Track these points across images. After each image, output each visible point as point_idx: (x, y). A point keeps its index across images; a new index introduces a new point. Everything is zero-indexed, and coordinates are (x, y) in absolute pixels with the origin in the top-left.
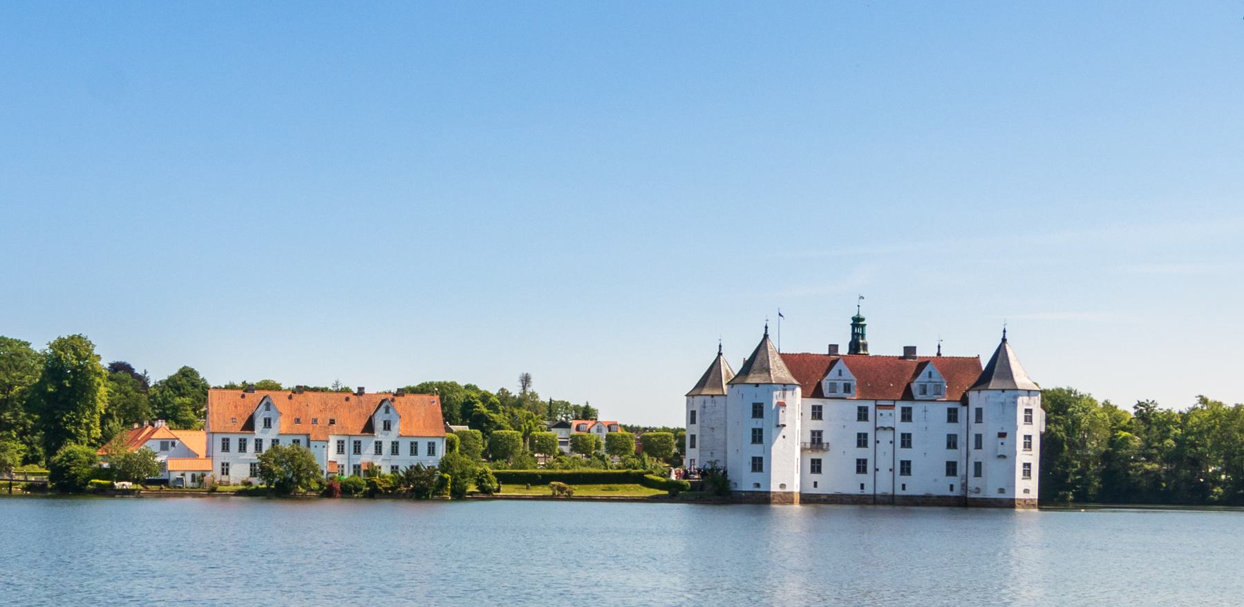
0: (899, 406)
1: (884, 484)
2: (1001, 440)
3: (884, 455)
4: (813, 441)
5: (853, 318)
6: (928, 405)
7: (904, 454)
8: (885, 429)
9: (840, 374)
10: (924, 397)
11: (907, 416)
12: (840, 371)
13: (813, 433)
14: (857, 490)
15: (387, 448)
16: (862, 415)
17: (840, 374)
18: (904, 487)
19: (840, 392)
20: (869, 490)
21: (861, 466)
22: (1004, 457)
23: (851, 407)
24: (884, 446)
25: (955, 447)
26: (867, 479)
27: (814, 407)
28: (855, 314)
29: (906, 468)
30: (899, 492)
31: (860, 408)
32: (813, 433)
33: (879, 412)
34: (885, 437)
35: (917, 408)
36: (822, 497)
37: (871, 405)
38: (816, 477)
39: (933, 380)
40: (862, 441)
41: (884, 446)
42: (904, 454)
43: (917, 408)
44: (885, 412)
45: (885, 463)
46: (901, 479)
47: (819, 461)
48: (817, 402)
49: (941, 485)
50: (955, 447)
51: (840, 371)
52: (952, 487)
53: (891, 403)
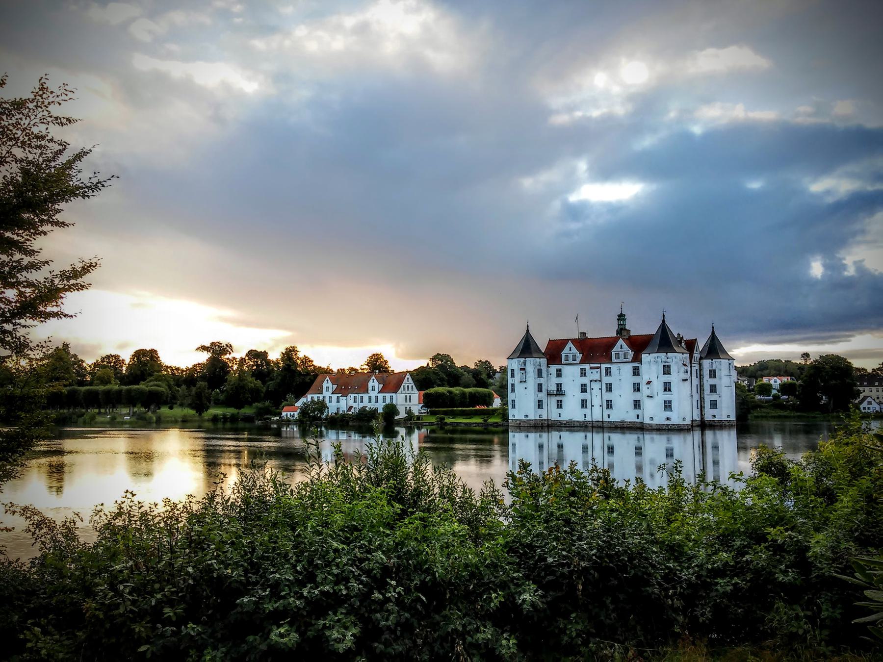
0: (604, 366)
1: (597, 414)
2: (648, 386)
3: (596, 398)
4: (558, 390)
5: (619, 316)
6: (621, 365)
7: (607, 396)
8: (596, 381)
9: (570, 350)
10: (618, 361)
11: (608, 373)
12: (570, 348)
13: (557, 385)
14: (581, 419)
15: (373, 399)
16: (583, 373)
17: (570, 350)
18: (609, 415)
19: (571, 361)
20: (589, 418)
21: (584, 404)
22: (652, 397)
23: (577, 369)
24: (596, 391)
25: (639, 391)
26: (587, 411)
27: (557, 370)
28: (619, 314)
29: (609, 404)
30: (606, 419)
31: (582, 370)
32: (557, 385)
33: (592, 370)
34: (596, 386)
35: (614, 368)
36: (563, 422)
37: (587, 367)
38: (560, 410)
39: (623, 350)
40: (583, 388)
41: (596, 391)
42: (607, 396)
43: (614, 368)
44: (594, 371)
45: (597, 401)
46: (607, 412)
47: (561, 401)
48: (559, 367)
49: (630, 416)
50: (639, 391)
51: (570, 348)
52: (638, 416)
53: (598, 365)
